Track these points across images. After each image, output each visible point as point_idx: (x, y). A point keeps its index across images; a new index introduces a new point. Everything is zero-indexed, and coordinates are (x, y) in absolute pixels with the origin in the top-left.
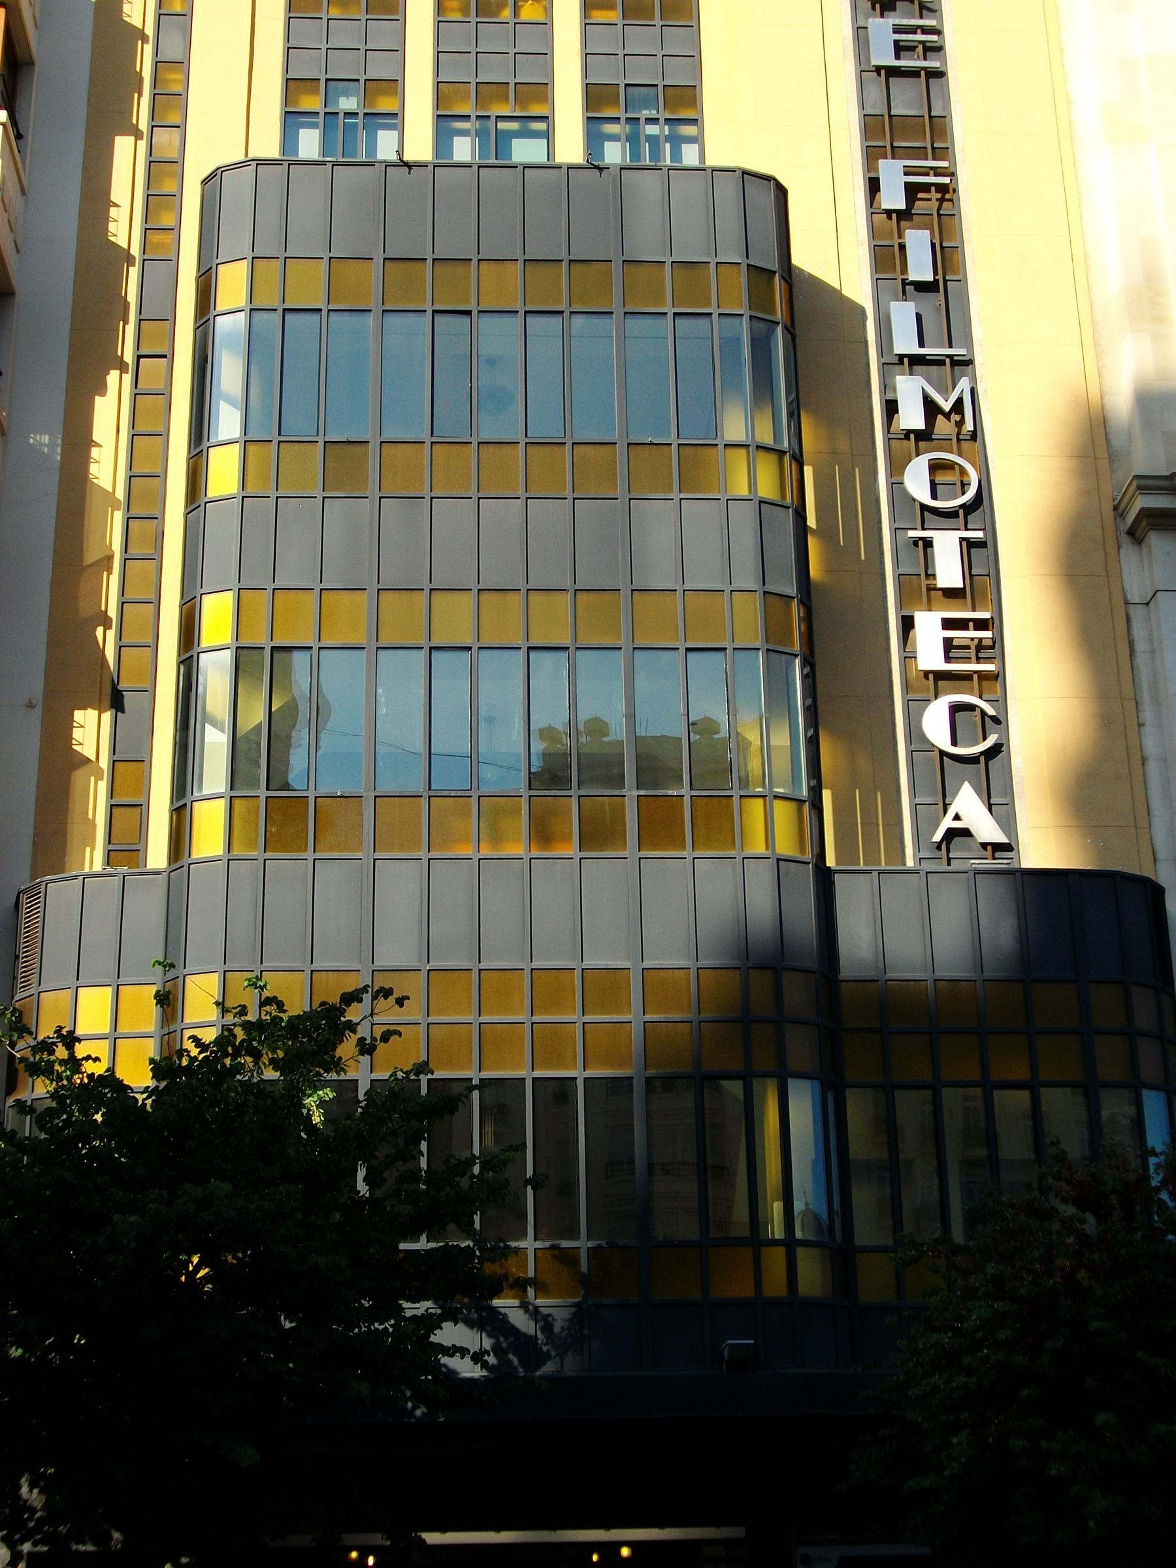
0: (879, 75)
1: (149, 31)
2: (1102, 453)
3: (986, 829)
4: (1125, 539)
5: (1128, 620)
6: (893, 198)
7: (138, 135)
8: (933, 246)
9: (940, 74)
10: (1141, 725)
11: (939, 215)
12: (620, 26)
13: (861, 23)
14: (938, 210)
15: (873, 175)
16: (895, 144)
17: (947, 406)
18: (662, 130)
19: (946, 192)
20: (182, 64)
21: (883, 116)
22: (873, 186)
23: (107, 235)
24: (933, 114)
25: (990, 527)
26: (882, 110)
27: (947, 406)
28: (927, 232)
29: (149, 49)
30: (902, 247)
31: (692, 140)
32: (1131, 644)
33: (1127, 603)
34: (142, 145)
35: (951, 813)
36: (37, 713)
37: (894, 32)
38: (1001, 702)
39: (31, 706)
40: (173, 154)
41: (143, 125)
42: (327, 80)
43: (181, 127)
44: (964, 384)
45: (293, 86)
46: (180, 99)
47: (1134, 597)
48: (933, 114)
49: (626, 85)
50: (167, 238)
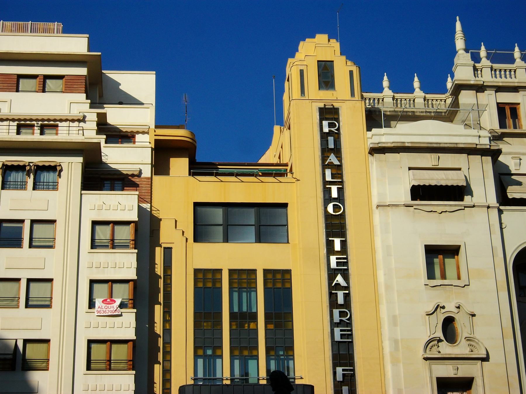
0: (337, 342)
1: (161, 335)
6: (339, 378)
7: (160, 364)
8: (349, 390)
9: (352, 342)
11: (350, 381)
12: (274, 330)
13: (332, 328)
14: (351, 379)
15: (335, 371)
16: (340, 362)
18: (285, 357)
19: (353, 376)
20: (170, 343)
21: (337, 354)
22: (335, 373)
23: (154, 392)
24: (350, 353)
26: (337, 352)
28: (347, 387)
29: (162, 339)
30: (342, 390)
31: (291, 359)
34: (161, 366)
37: (341, 332)
40: (169, 368)
41: (161, 361)
42: (204, 347)
43: (170, 361)
45: (196, 348)
46: (170, 353)
48: (350, 353)
49: (276, 347)
50: (168, 391)
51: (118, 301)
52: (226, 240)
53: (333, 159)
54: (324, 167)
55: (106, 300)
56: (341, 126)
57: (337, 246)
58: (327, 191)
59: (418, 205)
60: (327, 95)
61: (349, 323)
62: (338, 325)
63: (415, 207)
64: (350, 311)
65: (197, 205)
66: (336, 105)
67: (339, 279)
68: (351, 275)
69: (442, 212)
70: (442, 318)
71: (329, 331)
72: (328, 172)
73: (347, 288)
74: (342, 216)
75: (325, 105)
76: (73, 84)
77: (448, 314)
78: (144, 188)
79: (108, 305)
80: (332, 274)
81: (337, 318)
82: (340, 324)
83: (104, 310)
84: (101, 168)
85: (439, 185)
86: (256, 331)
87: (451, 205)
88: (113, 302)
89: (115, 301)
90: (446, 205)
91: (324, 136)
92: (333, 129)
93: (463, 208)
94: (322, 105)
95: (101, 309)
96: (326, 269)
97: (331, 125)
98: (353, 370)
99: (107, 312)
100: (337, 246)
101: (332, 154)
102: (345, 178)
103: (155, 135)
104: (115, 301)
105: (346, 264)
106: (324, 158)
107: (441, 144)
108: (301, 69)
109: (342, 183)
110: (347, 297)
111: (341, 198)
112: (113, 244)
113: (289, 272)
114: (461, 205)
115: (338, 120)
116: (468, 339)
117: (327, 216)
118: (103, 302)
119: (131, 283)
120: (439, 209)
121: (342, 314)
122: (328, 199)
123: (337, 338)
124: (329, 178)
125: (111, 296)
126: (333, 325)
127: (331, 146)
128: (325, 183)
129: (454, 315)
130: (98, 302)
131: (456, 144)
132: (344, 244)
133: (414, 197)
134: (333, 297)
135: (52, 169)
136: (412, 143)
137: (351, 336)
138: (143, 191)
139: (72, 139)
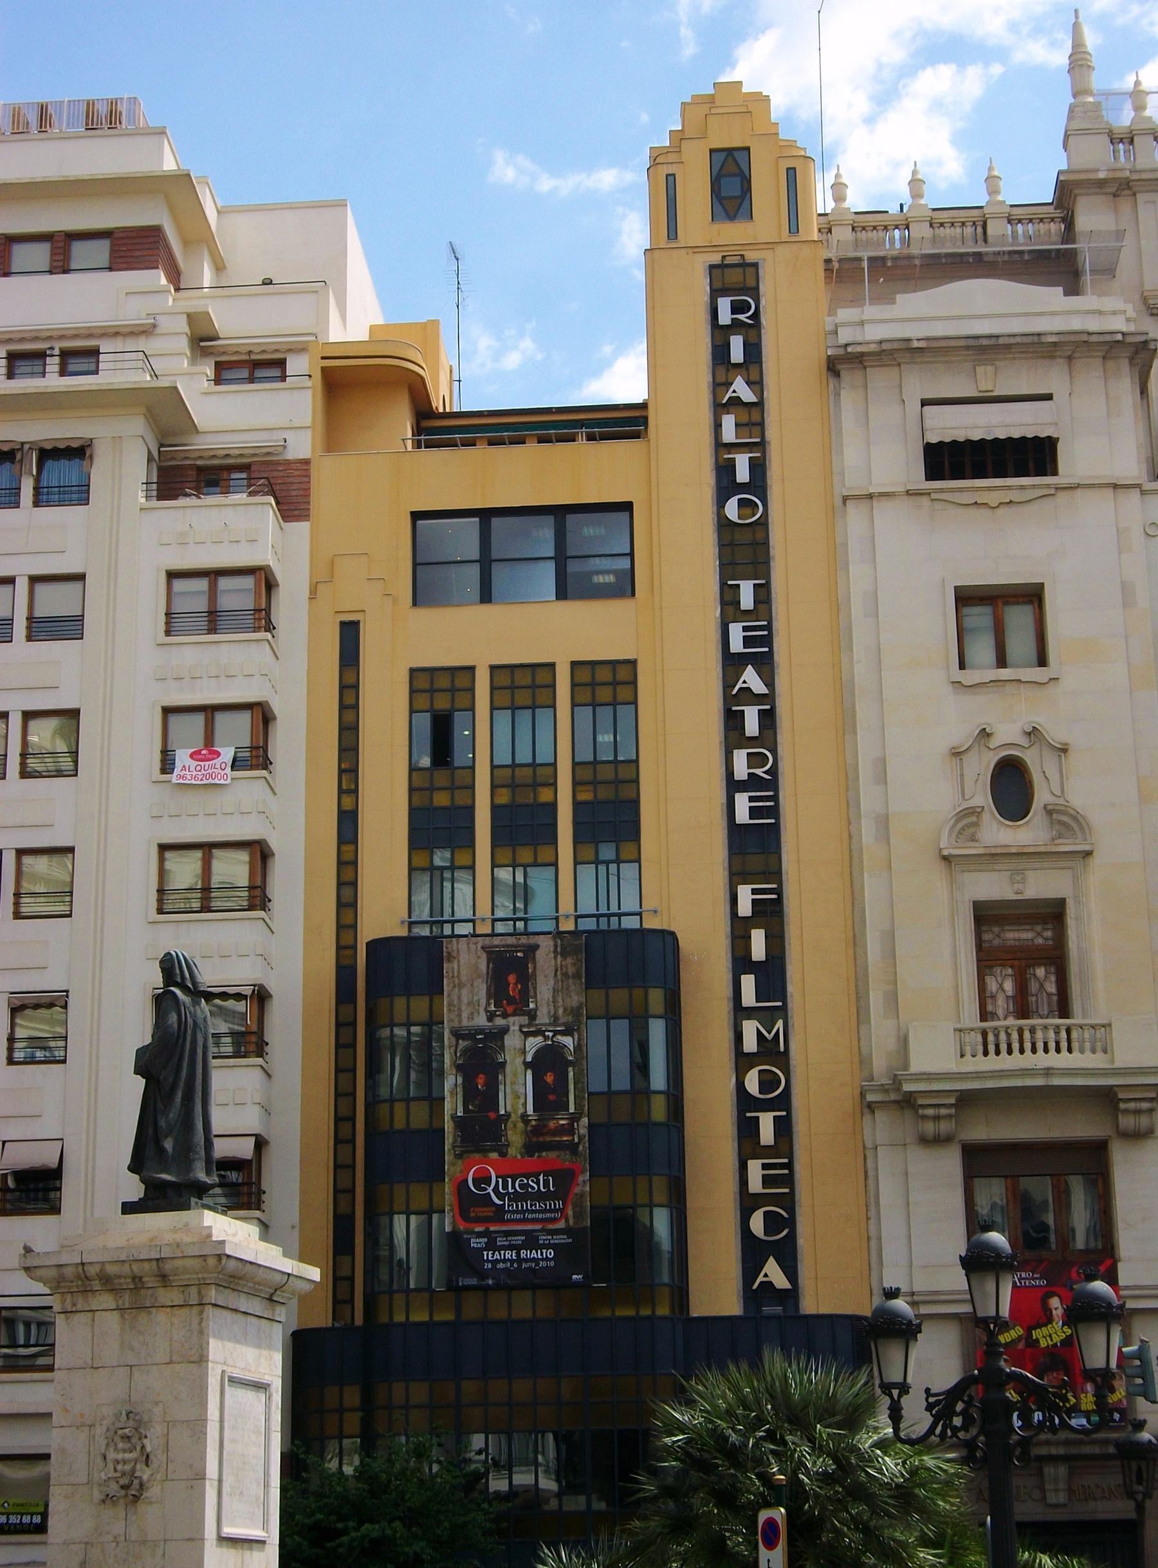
2: (856, 1060)
3: (780, 1281)
4: (866, 1110)
5: (865, 1158)
6: (745, 908)
10: (868, 1219)
17: (770, 1037)
25: (788, 1110)
27: (770, 1037)
32: (866, 1173)
33: (864, 1147)
35: (762, 1274)
36: (296, 1232)
37: (750, 801)
38: (791, 1210)
39: (293, 1227)
44: (780, 1024)
47: (869, 1145)
51: (227, 754)
52: (486, 596)
53: (741, 389)
54: (720, 409)
55: (198, 752)
56: (764, 307)
57: (747, 600)
58: (725, 470)
59: (941, 491)
60: (733, 234)
61: (771, 783)
62: (741, 786)
63: (933, 496)
64: (774, 752)
65: (416, 516)
66: (751, 257)
67: (751, 678)
68: (778, 667)
69: (1000, 504)
70: (992, 759)
71: (724, 800)
72: (729, 422)
73: (769, 698)
74: (763, 524)
75: (724, 257)
76: (133, 247)
77: (1005, 750)
78: (295, 487)
79: (202, 764)
80: (732, 663)
81: (741, 771)
82: (753, 782)
83: (194, 773)
84: (191, 445)
85: (989, 438)
86: (553, 807)
87: (1022, 488)
88: (215, 756)
89: (218, 754)
90: (1009, 488)
91: (720, 335)
92: (742, 317)
93: (1052, 491)
94: (716, 259)
95: (187, 773)
96: (720, 655)
97: (737, 308)
98: (779, 892)
99: (200, 777)
100: (747, 600)
101: (739, 377)
102: (771, 434)
103: (323, 358)
104: (218, 754)
105: (768, 641)
106: (719, 385)
107: (1000, 339)
108: (670, 172)
109: (762, 445)
110: (768, 718)
111: (758, 483)
112: (214, 621)
113: (633, 663)
114: (1048, 486)
115: (755, 292)
116: (1049, 811)
117: (724, 525)
118: (192, 756)
119: (256, 710)
120: (993, 498)
121: (755, 760)
122: (726, 485)
123: (742, 815)
124: (729, 434)
125: (209, 740)
126: (733, 786)
127: (737, 353)
128: (720, 446)
129: (1022, 752)
130: (182, 757)
131: (1039, 335)
132: (763, 594)
133: (933, 472)
134: (733, 720)
135: (79, 452)
136: (927, 339)
137: (774, 812)
138: (294, 493)
139: (112, 383)
